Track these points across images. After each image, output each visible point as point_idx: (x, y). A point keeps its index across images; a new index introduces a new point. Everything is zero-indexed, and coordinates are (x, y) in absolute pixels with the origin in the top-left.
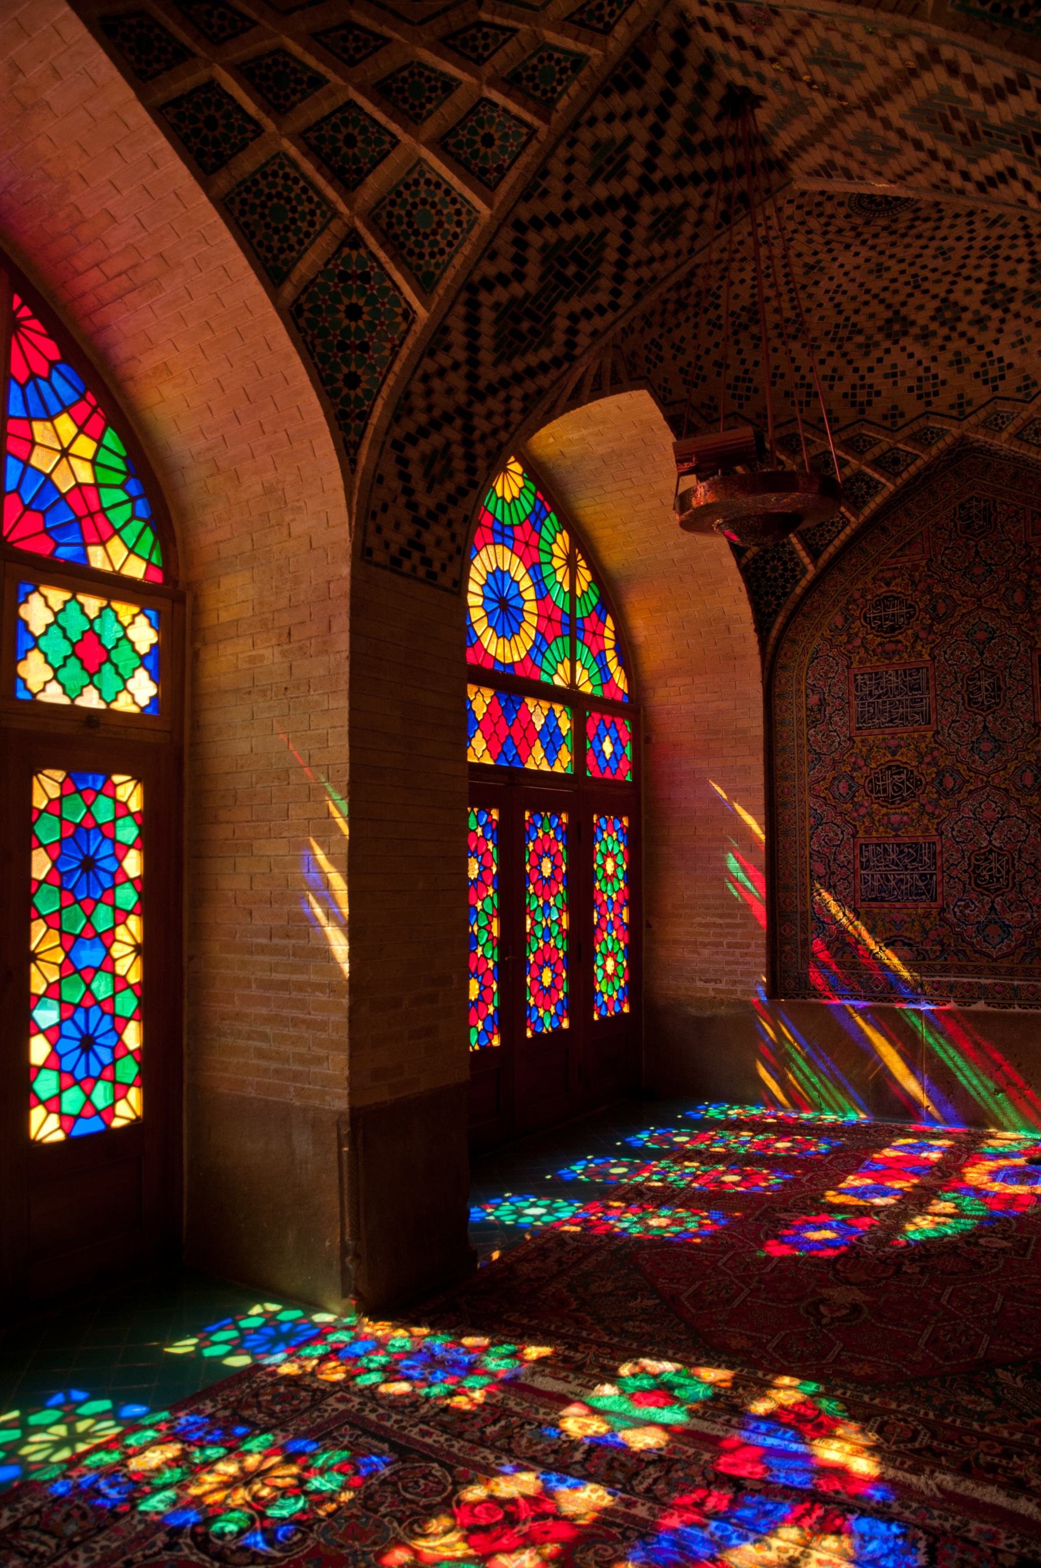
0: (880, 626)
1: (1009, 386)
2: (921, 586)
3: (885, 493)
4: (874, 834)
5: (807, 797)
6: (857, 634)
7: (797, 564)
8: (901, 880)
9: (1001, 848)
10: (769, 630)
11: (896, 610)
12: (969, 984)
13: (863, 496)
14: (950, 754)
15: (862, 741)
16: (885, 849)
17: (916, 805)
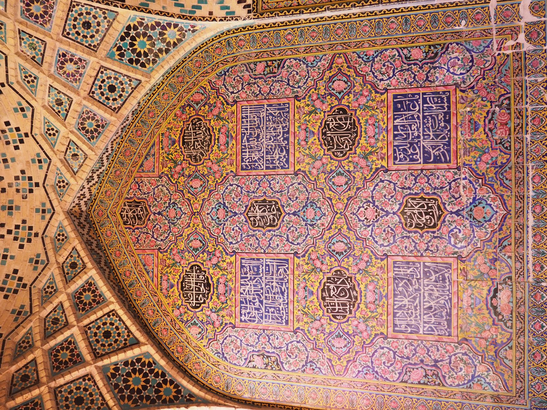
0: (204, 296)
1: (38, 175)
2: (177, 259)
4: (384, 317)
5: (347, 378)
7: (139, 360)
8: (430, 295)
9: (401, 204)
10: (191, 395)
11: (193, 280)
12: (535, 236)
13: (95, 296)
14: (314, 245)
15: (298, 321)
16: (400, 308)
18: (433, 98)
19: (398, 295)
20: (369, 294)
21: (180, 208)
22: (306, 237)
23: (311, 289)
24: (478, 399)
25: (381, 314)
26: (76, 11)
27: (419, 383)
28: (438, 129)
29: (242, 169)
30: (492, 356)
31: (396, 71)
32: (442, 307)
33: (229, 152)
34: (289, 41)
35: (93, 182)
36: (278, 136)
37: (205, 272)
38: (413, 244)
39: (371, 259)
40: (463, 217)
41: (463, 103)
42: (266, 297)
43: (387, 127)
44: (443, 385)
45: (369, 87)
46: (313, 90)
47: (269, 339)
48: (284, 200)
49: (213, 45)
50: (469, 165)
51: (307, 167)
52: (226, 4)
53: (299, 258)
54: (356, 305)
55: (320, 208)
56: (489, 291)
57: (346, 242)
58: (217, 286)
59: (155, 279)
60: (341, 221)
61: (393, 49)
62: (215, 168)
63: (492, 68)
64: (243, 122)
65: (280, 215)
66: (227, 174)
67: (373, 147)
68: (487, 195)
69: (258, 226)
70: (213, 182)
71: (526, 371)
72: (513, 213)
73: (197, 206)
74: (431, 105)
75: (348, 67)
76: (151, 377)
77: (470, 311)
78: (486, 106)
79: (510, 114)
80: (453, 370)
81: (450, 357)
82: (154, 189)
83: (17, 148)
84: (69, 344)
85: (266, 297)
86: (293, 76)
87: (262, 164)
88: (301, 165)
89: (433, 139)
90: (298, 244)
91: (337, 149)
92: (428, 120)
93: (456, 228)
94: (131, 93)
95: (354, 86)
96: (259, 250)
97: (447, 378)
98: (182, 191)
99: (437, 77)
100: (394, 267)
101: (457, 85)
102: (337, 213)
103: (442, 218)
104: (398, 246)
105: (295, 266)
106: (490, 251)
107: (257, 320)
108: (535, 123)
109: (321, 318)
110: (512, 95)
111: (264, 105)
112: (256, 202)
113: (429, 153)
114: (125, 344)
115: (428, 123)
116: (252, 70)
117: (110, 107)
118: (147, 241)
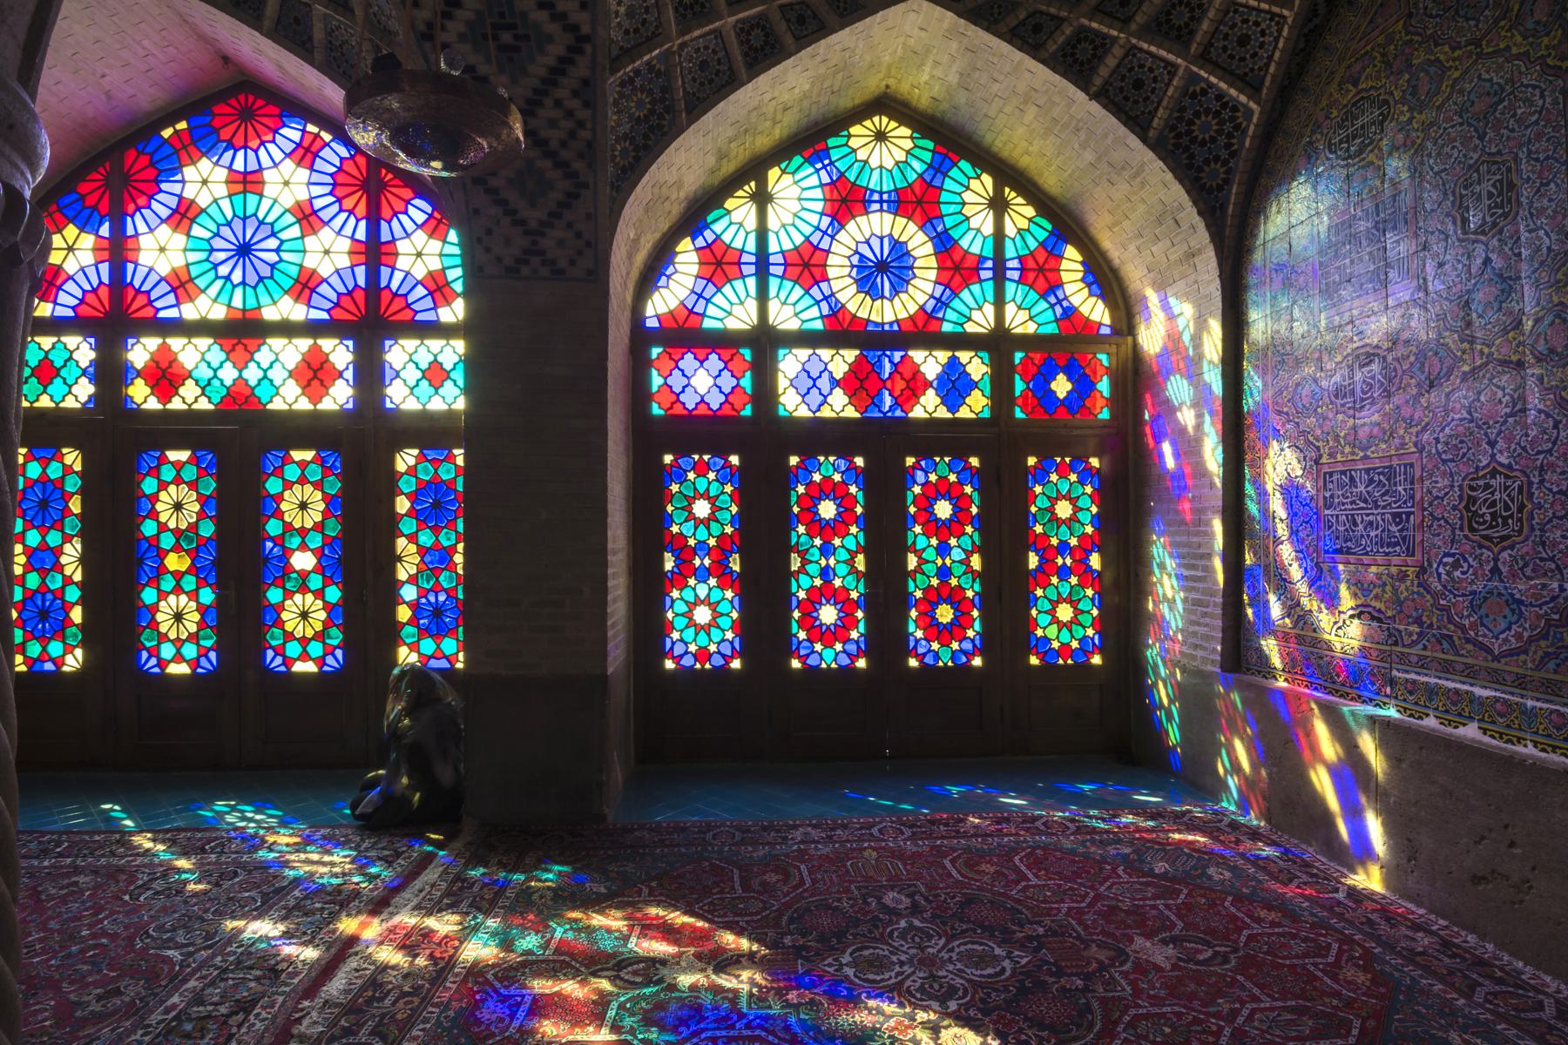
7: (1235, 109)
8: (1371, 523)
9: (1509, 467)
10: (1223, 207)
12: (1457, 691)
16: (1352, 478)
56: (1379, 611)
70: (1547, 47)
72: (1495, 665)
76: (1222, 140)
93: (1470, 566)
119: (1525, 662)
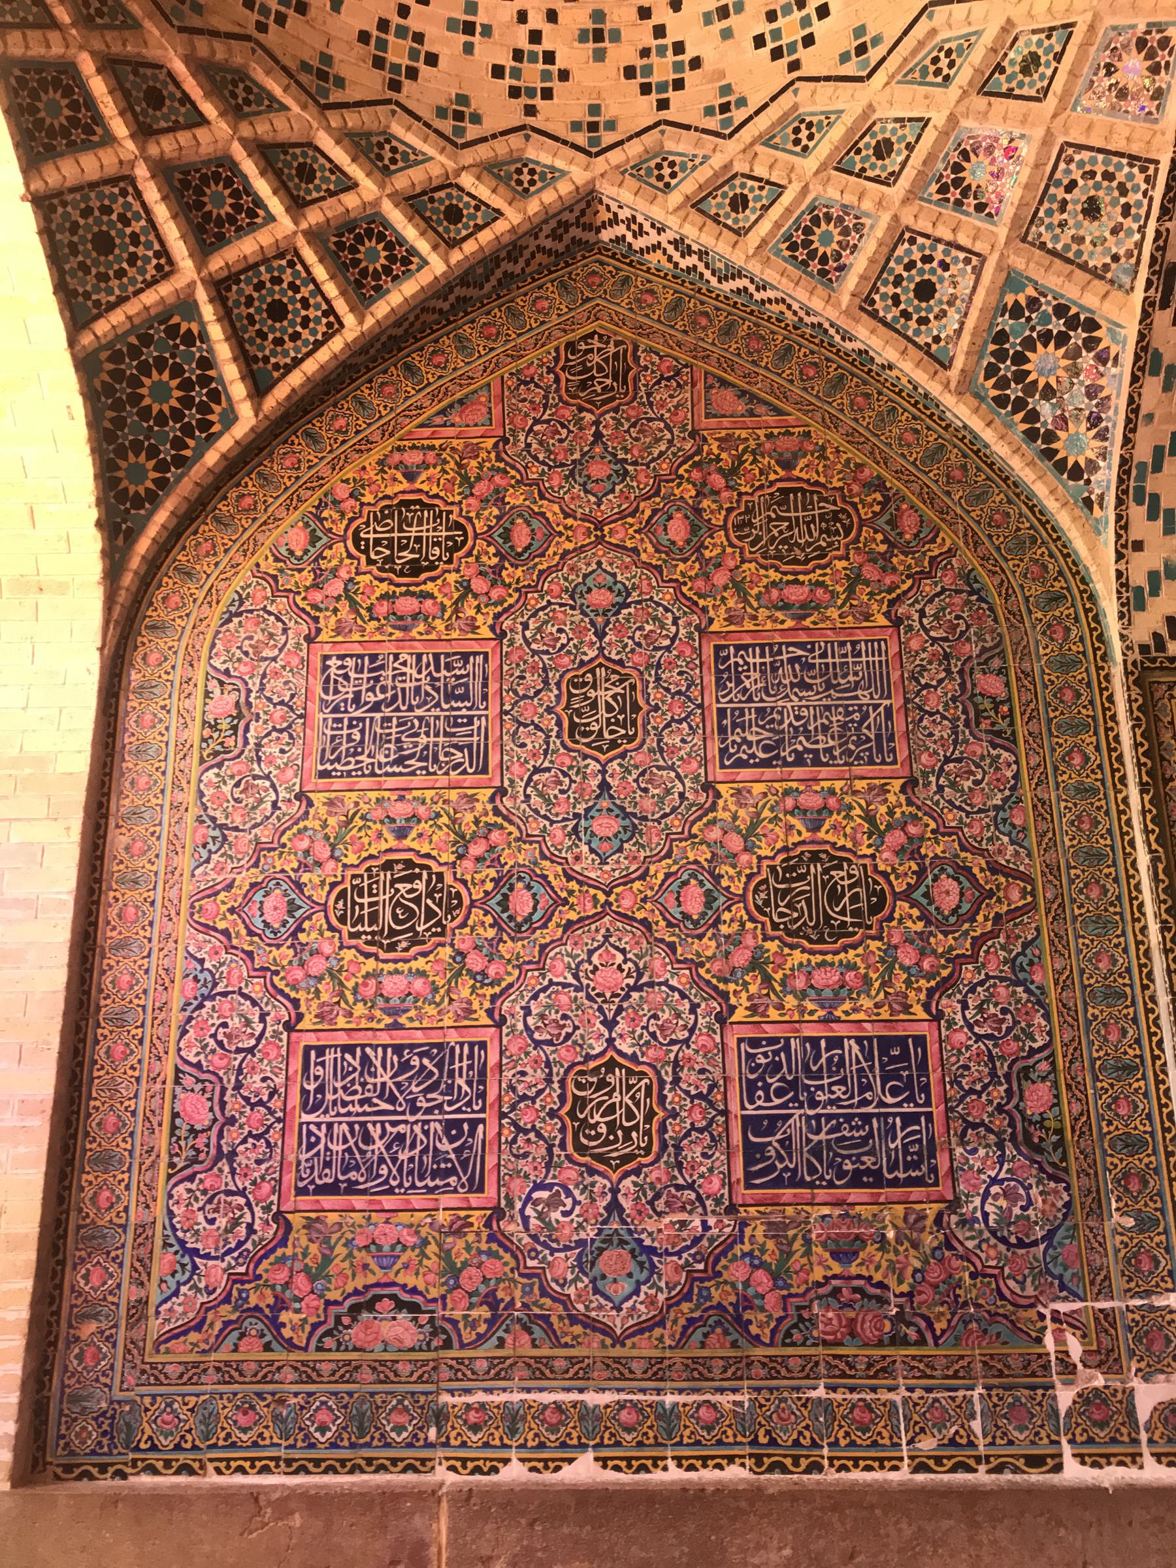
0: (389, 559)
1: (688, 104)
2: (481, 488)
3: (424, 278)
5: (183, 930)
6: (334, 572)
7: (215, 396)
8: (401, 1138)
9: (633, 1058)
10: (132, 536)
11: (425, 531)
12: (558, 1407)
15: (330, 803)
16: (365, 1060)
17: (446, 953)
18: (920, 1141)
19: (400, 1056)
20: (401, 982)
21: (613, 491)
22: (545, 817)
23: (413, 834)
24: (137, 1264)
25: (351, 1014)
26: (1130, 176)
27: (175, 1115)
28: (836, 1155)
29: (718, 648)
30: (246, 1300)
31: (990, 1043)
32: (369, 1170)
33: (763, 613)
34: (1067, 758)
35: (676, 256)
36: (808, 739)
37: (450, 561)
38: (532, 1092)
39: (491, 984)
40: (605, 1222)
41: (905, 1219)
42: (389, 719)
43: (838, 1020)
44: (170, 1177)
45: (945, 973)
46: (933, 825)
47: (281, 731)
48: (639, 758)
49: (1051, 556)
50: (742, 1236)
51: (726, 815)
52: (1165, 585)
53: (492, 799)
54: (373, 949)
55: (620, 850)
56: (414, 1291)
57: (535, 917)
58: (413, 594)
59: (427, 432)
60: (589, 905)
61: (1049, 1033)
62: (720, 578)
63: (1002, 1297)
64: (842, 644)
65: (599, 749)
66: (704, 610)
67: (783, 983)
68: (663, 1284)
69: (571, 695)
70: (683, 574)
71: (209, 1388)
72: (617, 1351)
73: (618, 534)
74: (900, 1135)
75: (998, 916)
76: (173, 429)
77: (360, 1241)
78: (900, 1282)
79: (880, 1344)
80: (210, 1201)
81: (242, 1193)
82: (661, 419)
83: (759, 41)
84: (250, 213)
85: (389, 719)
86: (972, 773)
87: (731, 700)
88: (731, 800)
89: (809, 1141)
90: (528, 797)
91: (776, 890)
92: (858, 1128)
93: (576, 1202)
94: (915, 344)
95: (945, 934)
96: (509, 698)
97: (188, 1185)
98: (657, 494)
99: (974, 1151)
100: (472, 1045)
101: (954, 1204)
102: (608, 894)
103: (602, 1168)
104: (527, 1054)
105: (470, 792)
106: (518, 1293)
107: (330, 698)
108: (857, 1411)
109: (338, 860)
110: (929, 1350)
111: (889, 697)
112: (633, 687)
113: (771, 1132)
114: (255, 359)
115: (852, 1128)
116: (986, 662)
117: (875, 289)
118: (525, 407)
119: (661, 1339)
